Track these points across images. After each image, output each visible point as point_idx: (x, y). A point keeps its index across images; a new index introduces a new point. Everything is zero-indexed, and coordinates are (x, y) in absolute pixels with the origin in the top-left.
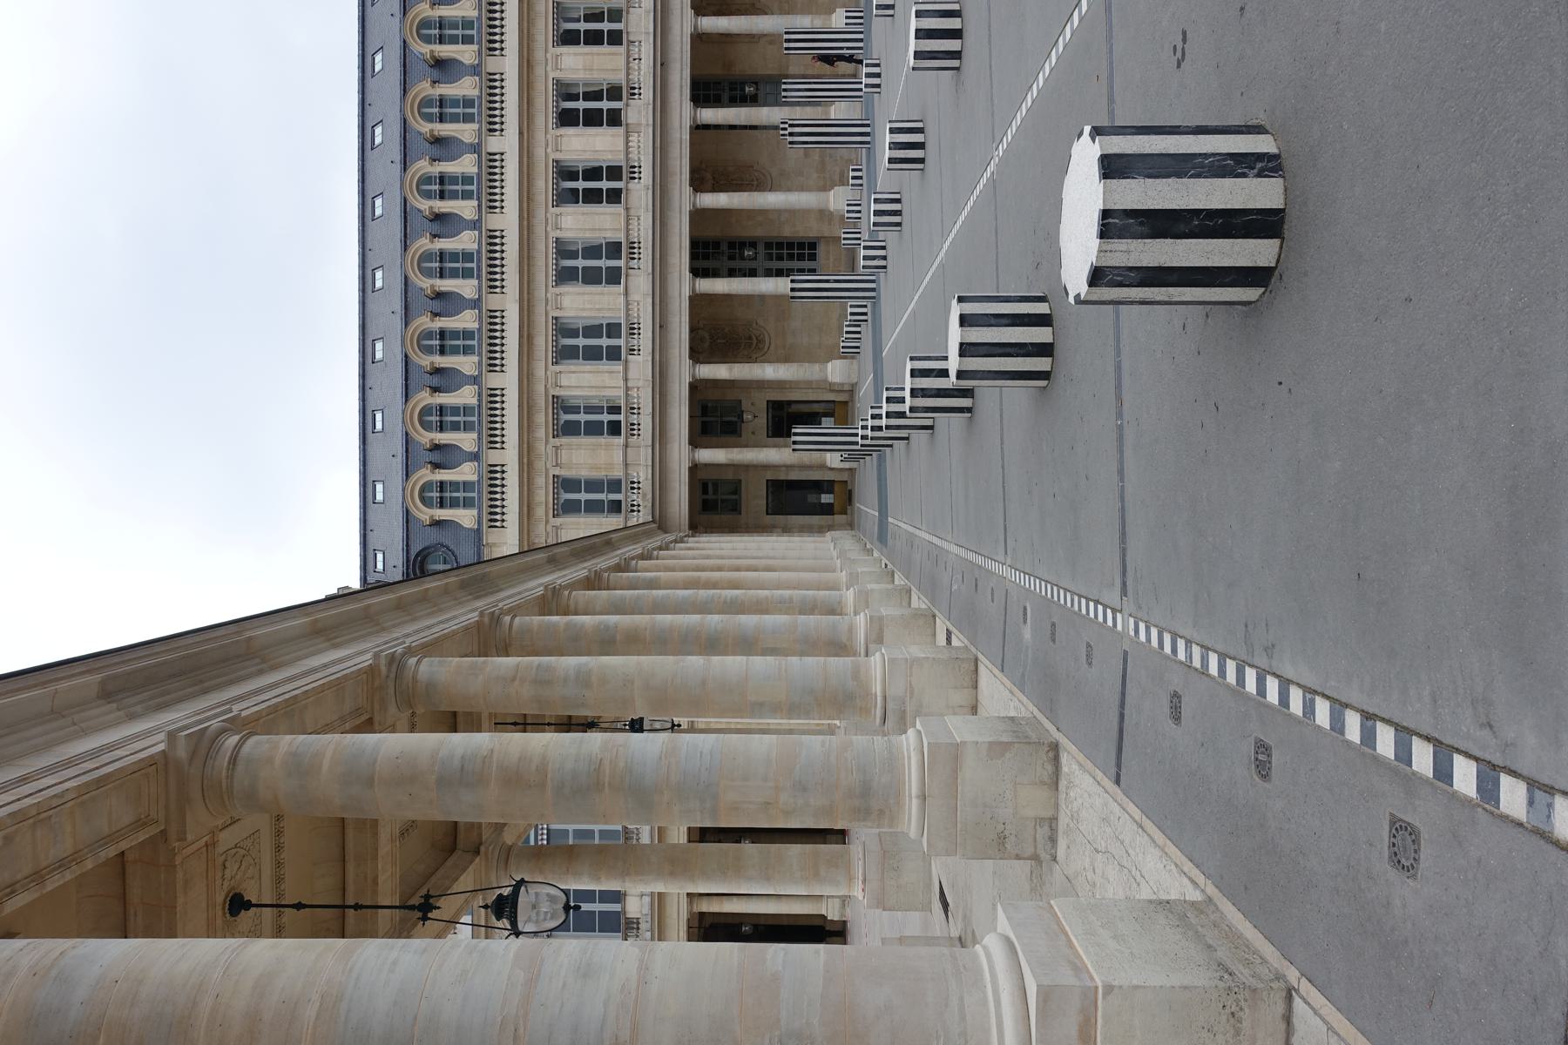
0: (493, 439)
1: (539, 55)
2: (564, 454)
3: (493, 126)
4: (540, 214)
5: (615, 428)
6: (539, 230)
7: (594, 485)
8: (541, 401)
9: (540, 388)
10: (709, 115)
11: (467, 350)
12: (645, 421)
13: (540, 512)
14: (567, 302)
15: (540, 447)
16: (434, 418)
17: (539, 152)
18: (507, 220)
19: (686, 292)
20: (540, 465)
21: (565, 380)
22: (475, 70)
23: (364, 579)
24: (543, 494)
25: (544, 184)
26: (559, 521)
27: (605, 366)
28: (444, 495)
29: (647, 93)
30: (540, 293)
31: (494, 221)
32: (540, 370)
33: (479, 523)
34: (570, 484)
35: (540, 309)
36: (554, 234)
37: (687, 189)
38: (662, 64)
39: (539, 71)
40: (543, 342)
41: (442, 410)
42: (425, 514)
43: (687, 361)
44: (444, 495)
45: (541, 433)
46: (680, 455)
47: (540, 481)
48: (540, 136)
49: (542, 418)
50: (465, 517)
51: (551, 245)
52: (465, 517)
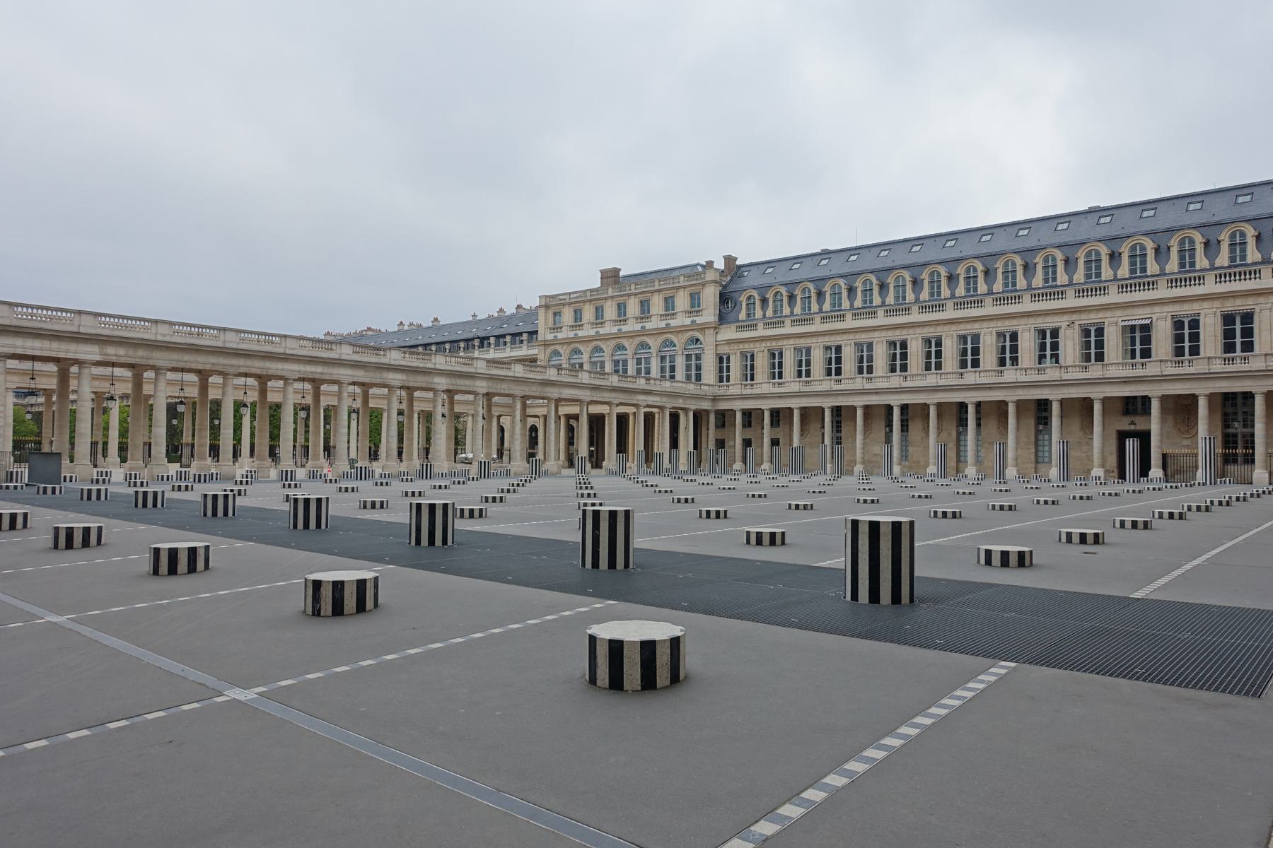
1: (918, 330)
4: (851, 336)
6: (845, 337)
8: (780, 343)
9: (785, 342)
10: (827, 414)
12: (748, 391)
15: (763, 345)
17: (877, 334)
23: (740, 267)
25: (863, 337)
29: (868, 386)
30: (820, 339)
32: (791, 342)
35: (814, 340)
36: (843, 343)
38: (877, 392)
39: (911, 331)
40: (802, 342)
46: (738, 406)
47: (752, 345)
48: (884, 334)
50: (743, 316)
52: (743, 316)
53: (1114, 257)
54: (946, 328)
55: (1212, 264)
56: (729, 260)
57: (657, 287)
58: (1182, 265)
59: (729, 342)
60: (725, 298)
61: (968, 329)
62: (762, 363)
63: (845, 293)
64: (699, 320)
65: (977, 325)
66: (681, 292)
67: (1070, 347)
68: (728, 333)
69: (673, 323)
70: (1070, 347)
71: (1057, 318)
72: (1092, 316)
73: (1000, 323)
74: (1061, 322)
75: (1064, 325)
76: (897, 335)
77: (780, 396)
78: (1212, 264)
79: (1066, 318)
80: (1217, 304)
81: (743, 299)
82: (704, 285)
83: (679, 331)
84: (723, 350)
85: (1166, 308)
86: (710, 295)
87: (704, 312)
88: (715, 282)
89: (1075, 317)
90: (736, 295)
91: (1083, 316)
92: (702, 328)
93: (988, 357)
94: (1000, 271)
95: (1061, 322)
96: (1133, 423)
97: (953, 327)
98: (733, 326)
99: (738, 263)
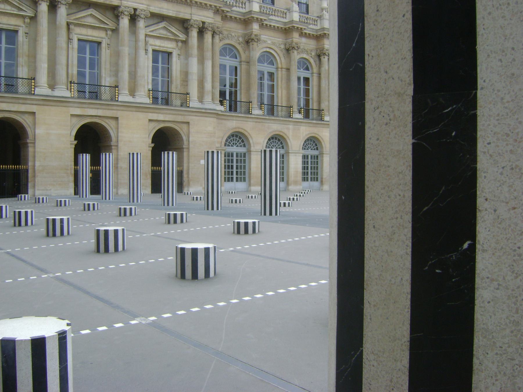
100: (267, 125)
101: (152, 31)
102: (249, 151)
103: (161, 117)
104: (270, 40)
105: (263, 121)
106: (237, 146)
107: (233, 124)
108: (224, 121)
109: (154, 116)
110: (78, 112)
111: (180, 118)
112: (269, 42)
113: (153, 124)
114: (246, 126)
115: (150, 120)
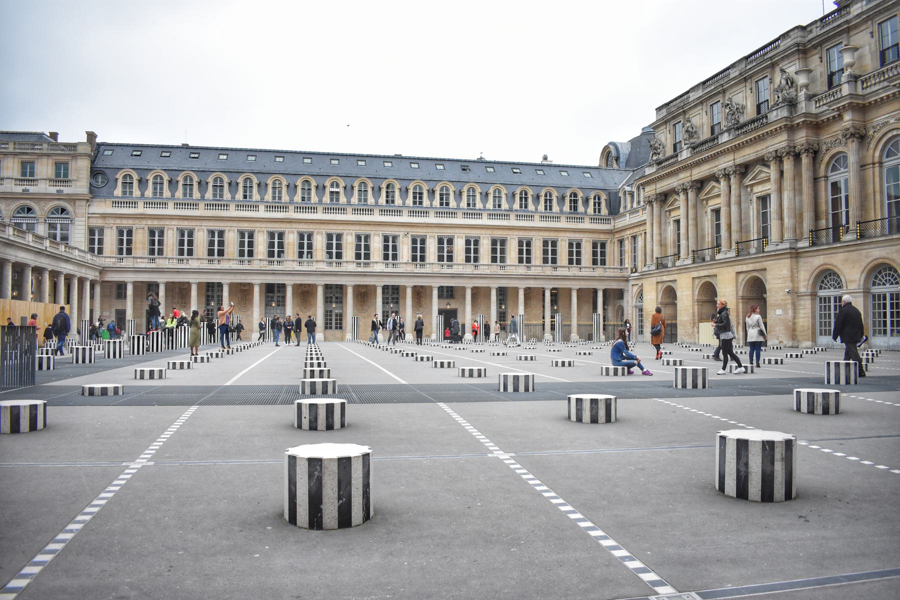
0: (147, 204)
2: (141, 231)
3: (269, 208)
4: (235, 224)
5: (152, 252)
6: (229, 224)
7: (129, 242)
8: (162, 223)
9: (167, 222)
11: (185, 195)
13: (118, 221)
14: (201, 233)
15: (144, 222)
16: (159, 181)
17: (258, 225)
18: (233, 212)
19: (191, 281)
20: (137, 221)
21: (170, 232)
22: (291, 201)
24: (126, 223)
25: (246, 226)
26: (115, 228)
27: (176, 248)
28: (128, 184)
30: (204, 223)
31: (232, 206)
32: (174, 222)
33: (115, 197)
34: (130, 233)
35: (198, 223)
36: (227, 229)
37: (229, 282)
38: (274, 273)
39: (288, 225)
40: (186, 224)
41: (162, 184)
42: (120, 176)
43: (165, 281)
44: (128, 184)
45: (149, 222)
48: (264, 225)
49: (155, 223)
50: (118, 192)
51: (222, 228)
52: (118, 192)
53: (432, 192)
54: (317, 226)
55: (485, 207)
56: (91, 136)
57: (11, 150)
58: (469, 205)
59: (104, 216)
60: (95, 172)
61: (334, 229)
62: (141, 239)
63: (226, 186)
64: (66, 190)
65: (341, 227)
66: (44, 160)
67: (405, 251)
68: (101, 207)
69: (32, 189)
70: (405, 251)
71: (396, 229)
72: (419, 230)
73: (358, 227)
74: (400, 232)
75: (402, 234)
76: (277, 228)
77: (178, 271)
78: (485, 207)
79: (402, 229)
80: (489, 232)
81: (120, 176)
82: (75, 157)
83: (41, 198)
84: (98, 223)
85: (462, 231)
86: (81, 168)
87: (73, 184)
88: (86, 155)
89: (408, 229)
90: (107, 171)
91: (414, 230)
92: (73, 199)
93: (349, 253)
94: (356, 189)
95: (400, 232)
96: (448, 304)
97: (323, 226)
98: (109, 202)
99: (98, 140)
100: (864, 251)
101: (753, 179)
102: (813, 295)
103: (745, 268)
104: (893, 117)
105: (859, 248)
106: (892, 284)
107: (818, 261)
108: (810, 259)
109: (739, 268)
110: (695, 274)
111: (758, 266)
112: (892, 121)
113: (742, 276)
114: (838, 260)
115: (738, 273)
